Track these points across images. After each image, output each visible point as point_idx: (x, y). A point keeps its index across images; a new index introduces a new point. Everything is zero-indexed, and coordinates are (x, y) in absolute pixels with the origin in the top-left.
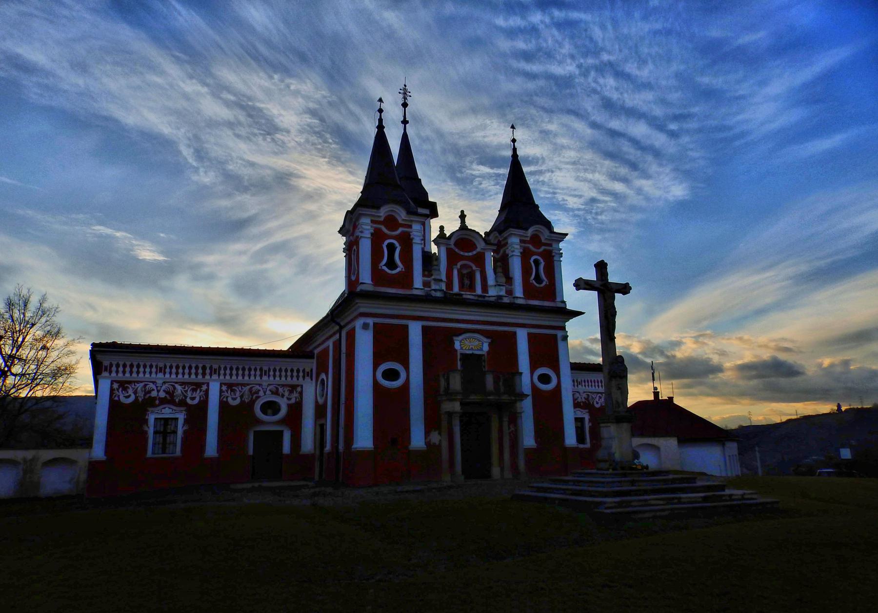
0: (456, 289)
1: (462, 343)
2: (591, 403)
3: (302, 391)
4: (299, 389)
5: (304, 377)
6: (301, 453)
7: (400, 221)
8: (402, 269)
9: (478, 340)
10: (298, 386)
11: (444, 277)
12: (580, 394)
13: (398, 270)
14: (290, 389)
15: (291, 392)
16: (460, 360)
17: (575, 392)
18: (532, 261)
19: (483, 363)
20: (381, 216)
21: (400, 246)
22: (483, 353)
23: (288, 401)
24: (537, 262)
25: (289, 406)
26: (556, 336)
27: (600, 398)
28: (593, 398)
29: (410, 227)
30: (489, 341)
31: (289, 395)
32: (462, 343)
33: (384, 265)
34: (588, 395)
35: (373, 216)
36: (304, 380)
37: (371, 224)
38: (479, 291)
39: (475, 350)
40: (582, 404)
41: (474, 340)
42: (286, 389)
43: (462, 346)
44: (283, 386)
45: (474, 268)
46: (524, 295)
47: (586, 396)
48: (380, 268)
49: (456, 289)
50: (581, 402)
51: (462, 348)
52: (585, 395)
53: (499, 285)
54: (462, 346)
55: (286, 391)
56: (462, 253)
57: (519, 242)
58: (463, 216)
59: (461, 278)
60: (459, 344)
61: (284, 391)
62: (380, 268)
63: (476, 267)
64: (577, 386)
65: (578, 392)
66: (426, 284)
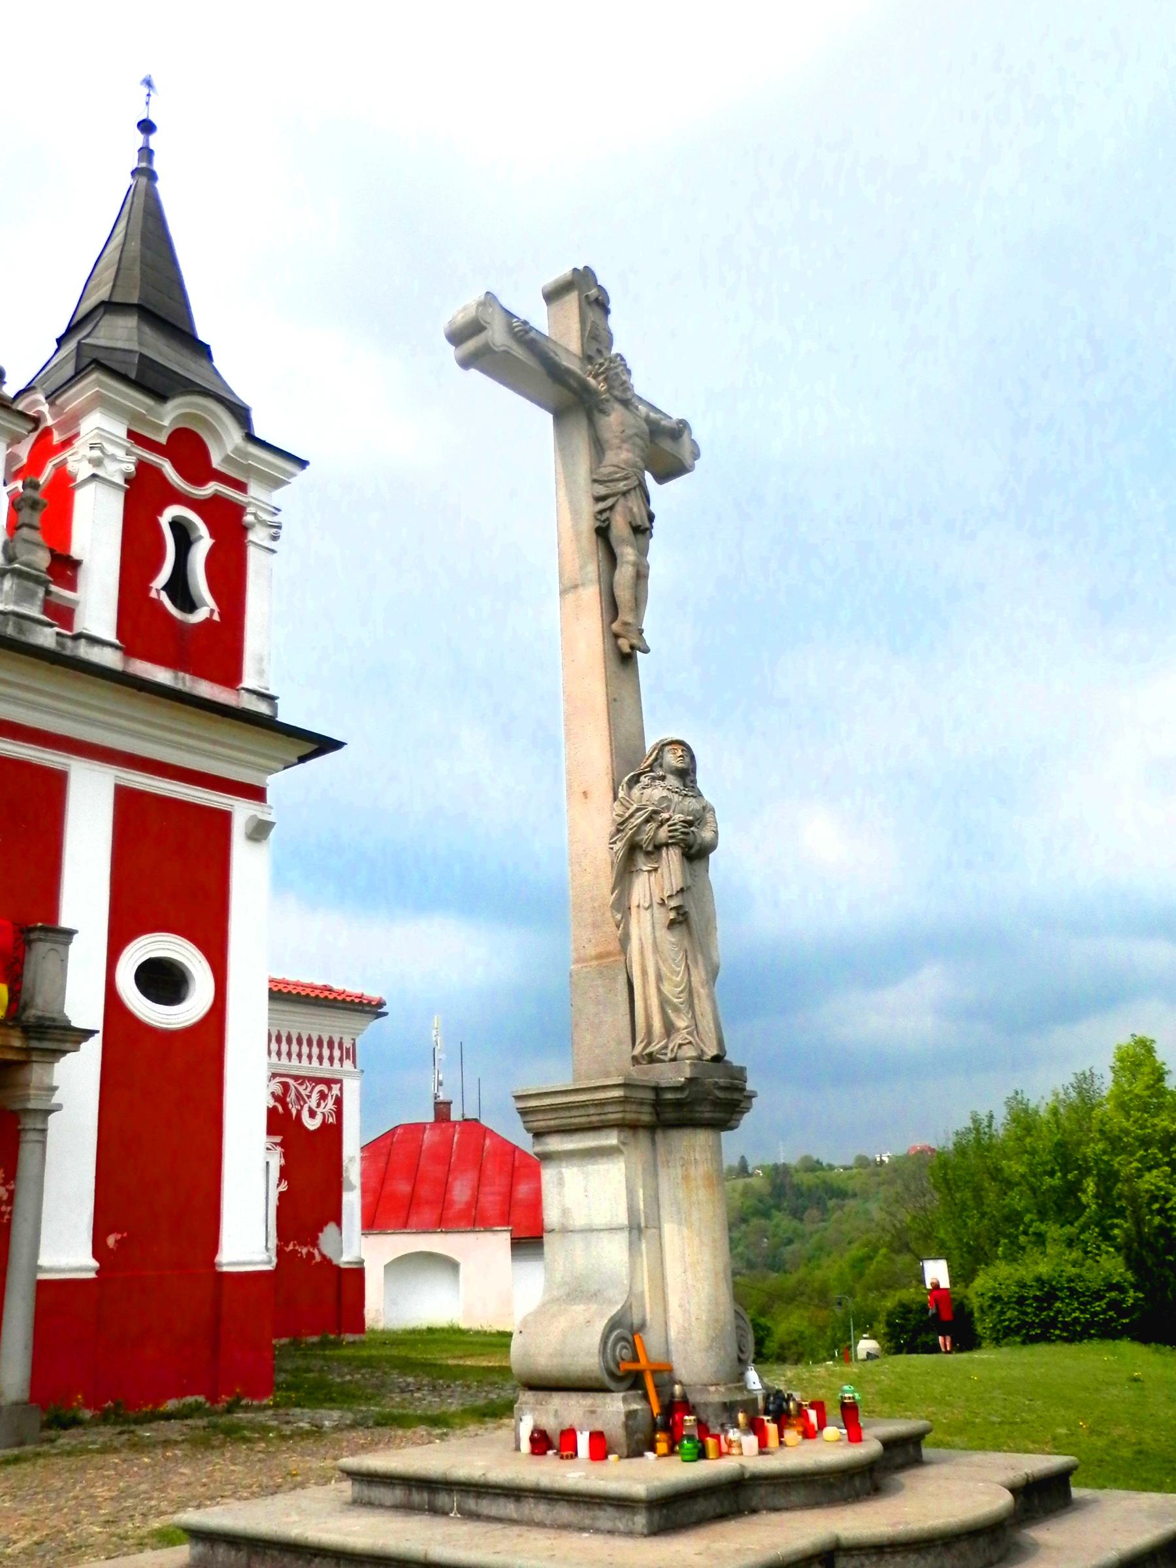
2: (294, 1112)
18: (165, 520)
27: (323, 1096)
28: (299, 1097)
34: (286, 1086)
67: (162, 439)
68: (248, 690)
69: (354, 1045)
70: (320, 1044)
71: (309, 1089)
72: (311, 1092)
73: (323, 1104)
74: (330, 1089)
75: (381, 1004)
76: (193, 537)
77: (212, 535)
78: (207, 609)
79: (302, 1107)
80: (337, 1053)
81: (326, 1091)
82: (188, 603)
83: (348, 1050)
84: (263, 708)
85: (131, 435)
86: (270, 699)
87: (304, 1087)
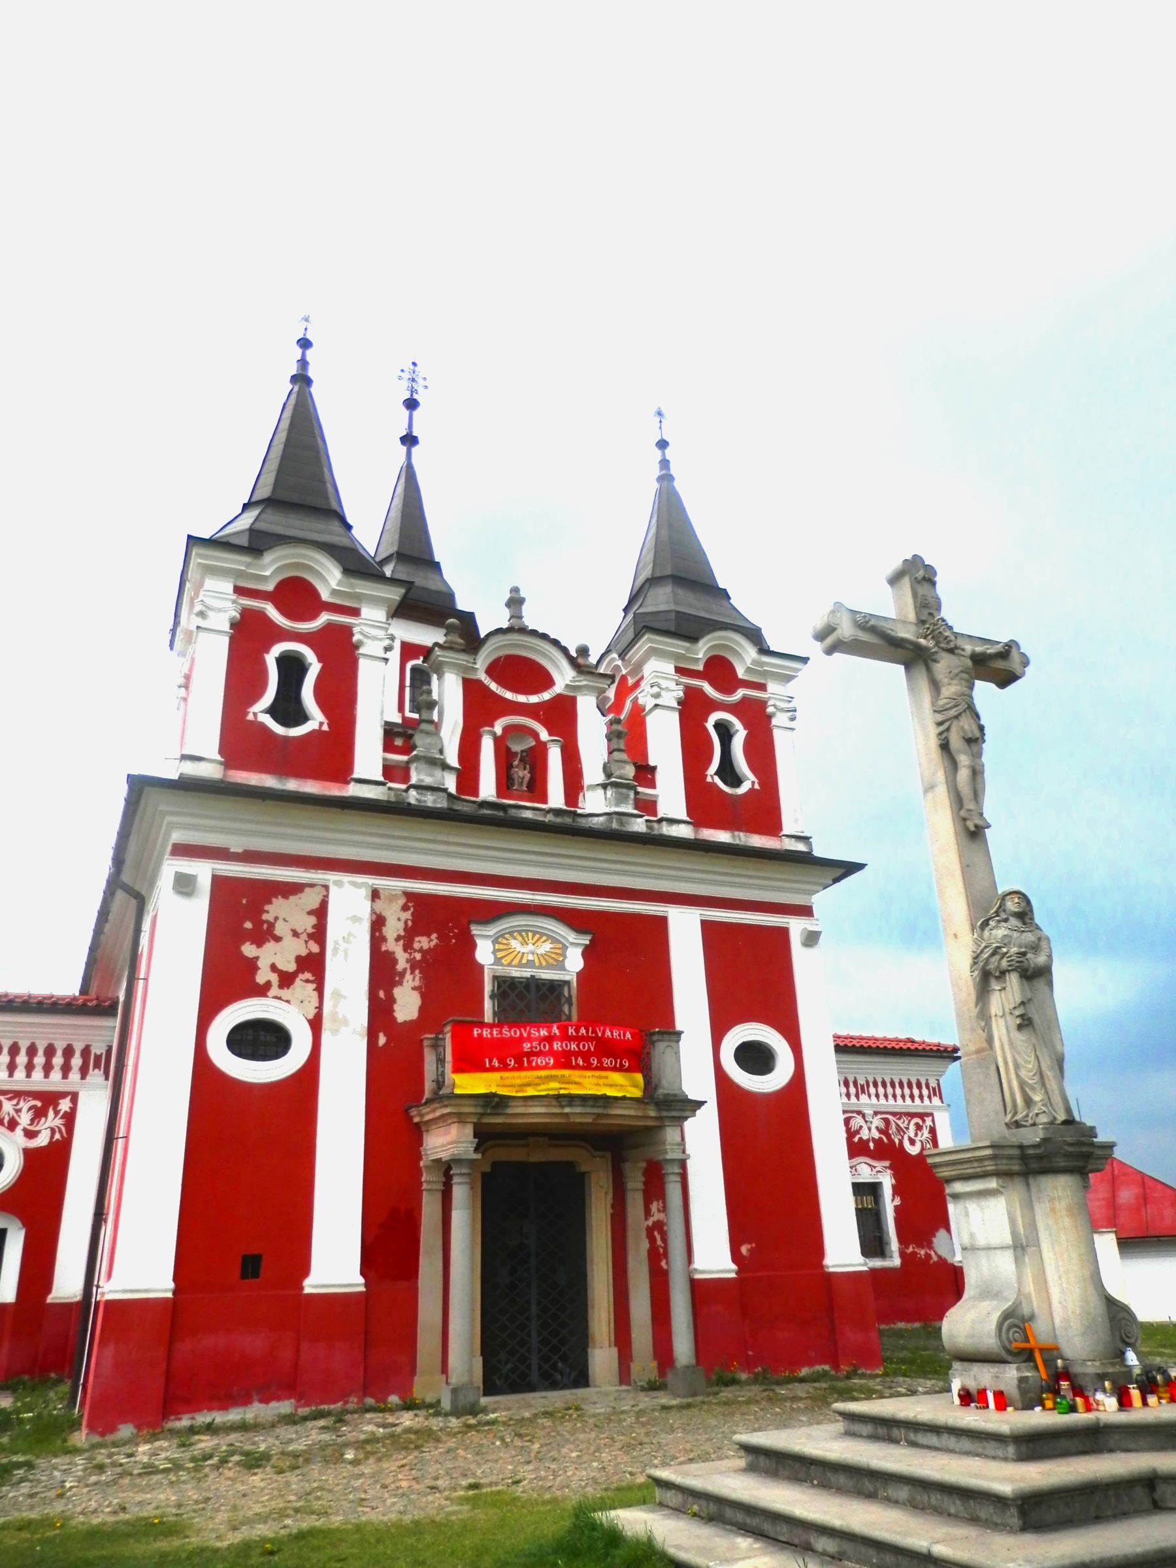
0: (488, 788)
1: (497, 946)
2: (897, 1141)
3: (73, 1110)
4: (65, 1105)
5: (84, 1072)
6: (50, 1299)
7: (325, 596)
8: (321, 724)
9: (549, 937)
10: (63, 1095)
11: (452, 759)
12: (864, 1116)
14: (39, 1104)
15: (39, 1114)
16: (492, 997)
17: (852, 1112)
18: (710, 725)
19: (566, 1009)
21: (319, 661)
22: (567, 978)
23: (25, 1139)
24: (724, 731)
25: (28, 1153)
26: (782, 934)
27: (919, 1127)
28: (899, 1128)
29: (355, 612)
30: (585, 940)
31: (32, 1121)
32: (497, 946)
33: (262, 712)
34: (887, 1121)
36: (83, 1077)
37: (234, 597)
38: (556, 797)
39: (540, 967)
40: (871, 1145)
41: (537, 936)
42: (25, 1105)
43: (499, 955)
44: (17, 1095)
45: (544, 735)
46: (688, 815)
47: (882, 1125)
48: (250, 717)
49: (488, 788)
50: (868, 1140)
51: (498, 961)
52: (877, 1122)
53: (616, 785)
54: (499, 955)
55: (25, 1110)
56: (509, 695)
57: (673, 672)
58: (515, 602)
59: (504, 758)
60: (492, 949)
61: (18, 1111)
62: (250, 717)
63: (550, 735)
64: (857, 1096)
65: (859, 1113)
66: (390, 771)
67: (700, 667)
68: (787, 836)
69: (939, 1085)
70: (910, 1085)
71: (906, 1122)
72: (908, 1124)
73: (920, 1134)
74: (924, 1121)
75: (956, 1050)
76: (732, 732)
77: (745, 728)
78: (750, 782)
79: (903, 1137)
80: (925, 1092)
81: (921, 1123)
82: (736, 781)
83: (934, 1089)
84: (801, 847)
85: (679, 670)
86: (805, 839)
87: (902, 1120)
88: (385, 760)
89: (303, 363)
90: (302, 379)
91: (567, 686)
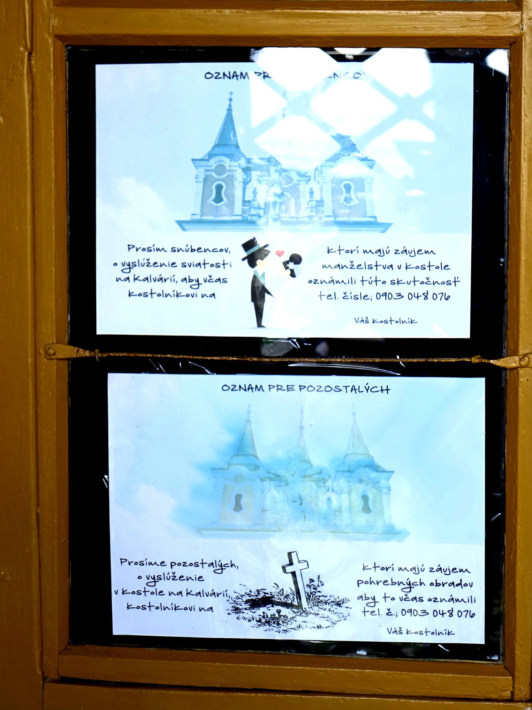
7: (227, 168)
8: (226, 201)
13: (223, 202)
20: (211, 166)
33: (211, 200)
35: (206, 166)
62: (208, 202)
66: (243, 212)
88: (242, 209)
89: (230, 105)
90: (230, 110)
91: (297, 181)
